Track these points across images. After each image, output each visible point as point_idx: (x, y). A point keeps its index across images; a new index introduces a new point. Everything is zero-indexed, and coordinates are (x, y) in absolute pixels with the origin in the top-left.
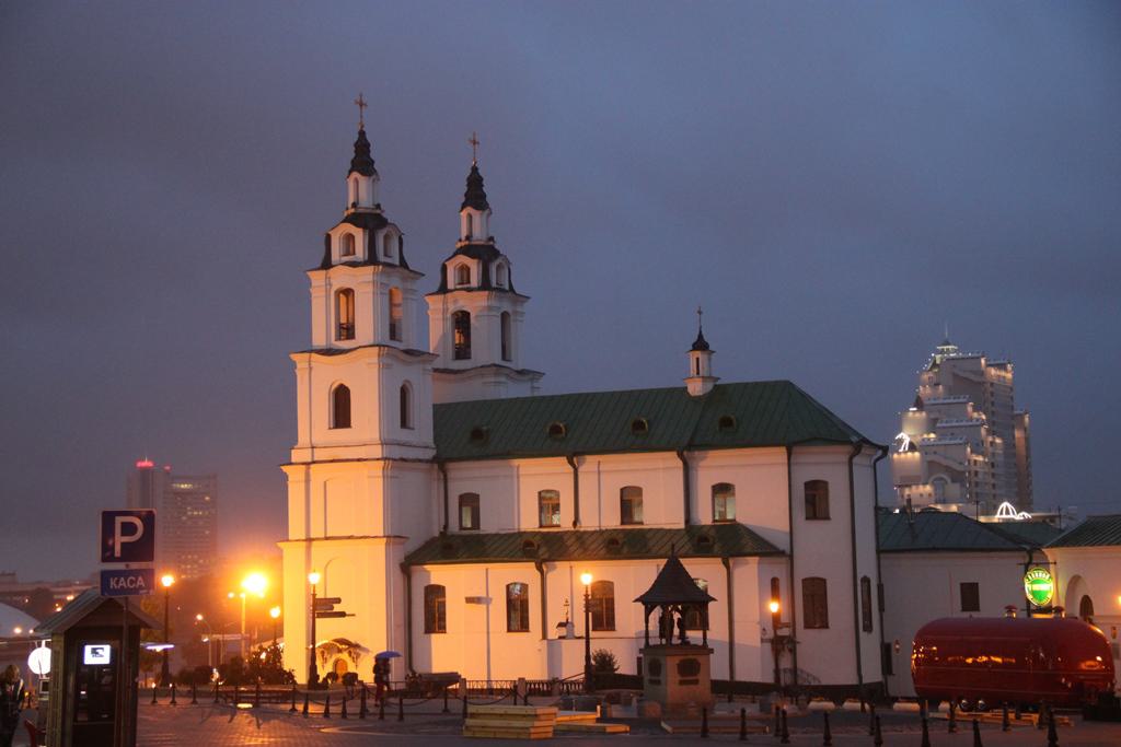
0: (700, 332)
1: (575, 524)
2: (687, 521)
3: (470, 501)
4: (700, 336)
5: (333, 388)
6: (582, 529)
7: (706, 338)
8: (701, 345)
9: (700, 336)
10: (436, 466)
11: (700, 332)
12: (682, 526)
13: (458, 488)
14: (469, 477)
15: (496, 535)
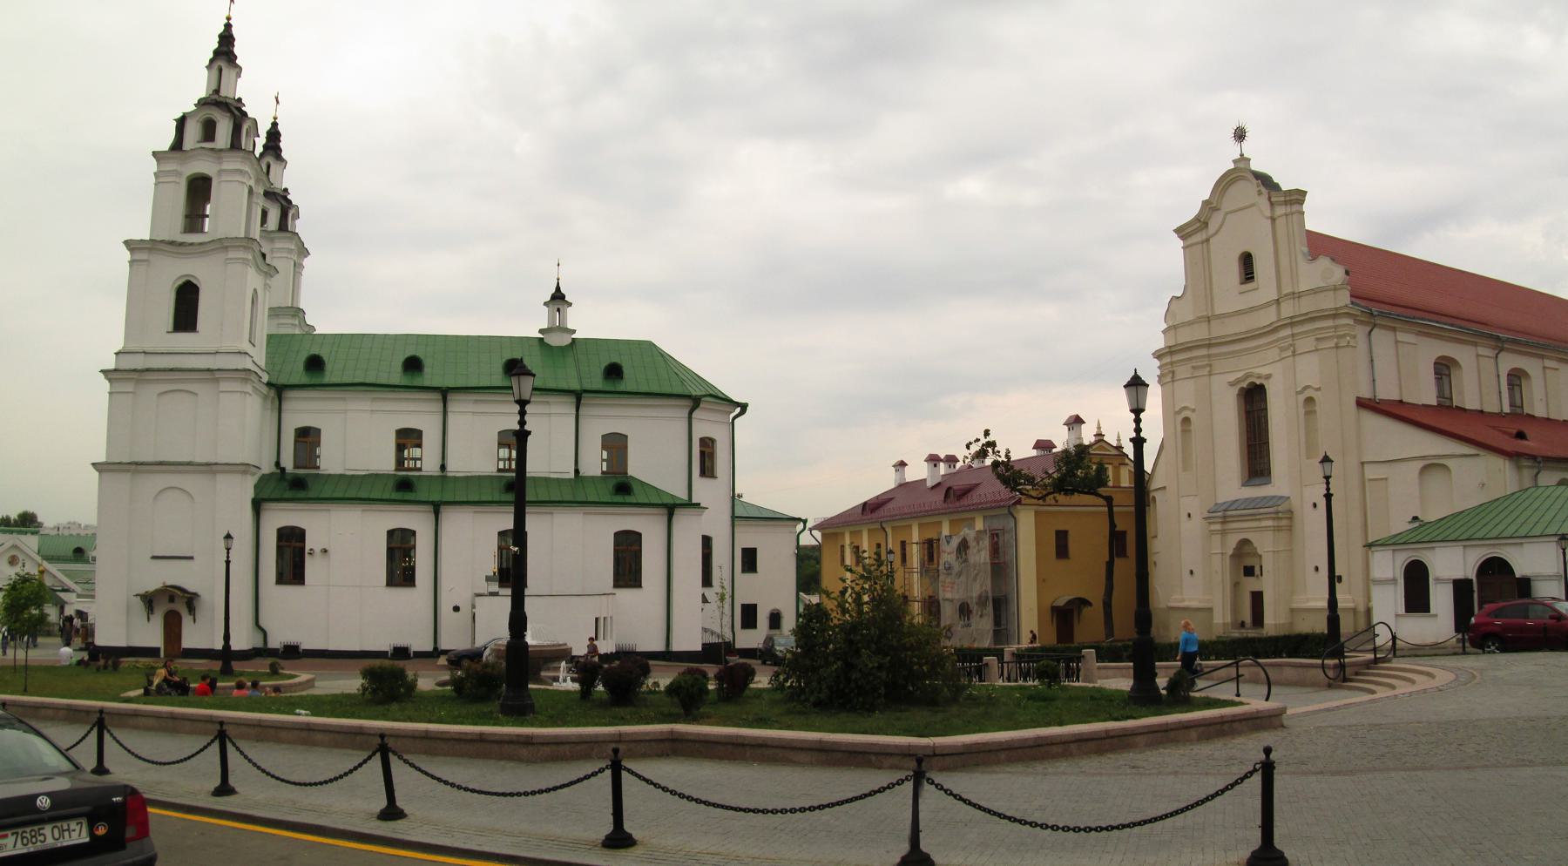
0: (558, 283)
1: (443, 467)
2: (577, 471)
3: (307, 437)
4: (558, 288)
5: (180, 282)
6: (449, 474)
7: (563, 290)
8: (558, 297)
9: (558, 288)
10: (273, 393)
11: (558, 283)
12: (572, 475)
13: (294, 420)
14: (302, 411)
15: (341, 476)
